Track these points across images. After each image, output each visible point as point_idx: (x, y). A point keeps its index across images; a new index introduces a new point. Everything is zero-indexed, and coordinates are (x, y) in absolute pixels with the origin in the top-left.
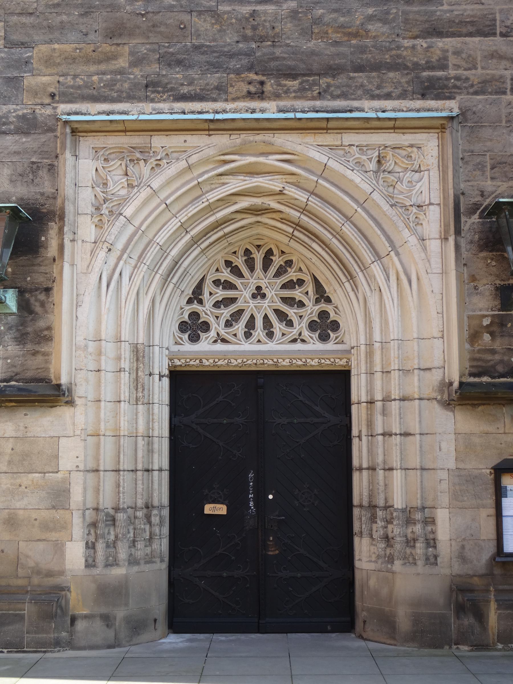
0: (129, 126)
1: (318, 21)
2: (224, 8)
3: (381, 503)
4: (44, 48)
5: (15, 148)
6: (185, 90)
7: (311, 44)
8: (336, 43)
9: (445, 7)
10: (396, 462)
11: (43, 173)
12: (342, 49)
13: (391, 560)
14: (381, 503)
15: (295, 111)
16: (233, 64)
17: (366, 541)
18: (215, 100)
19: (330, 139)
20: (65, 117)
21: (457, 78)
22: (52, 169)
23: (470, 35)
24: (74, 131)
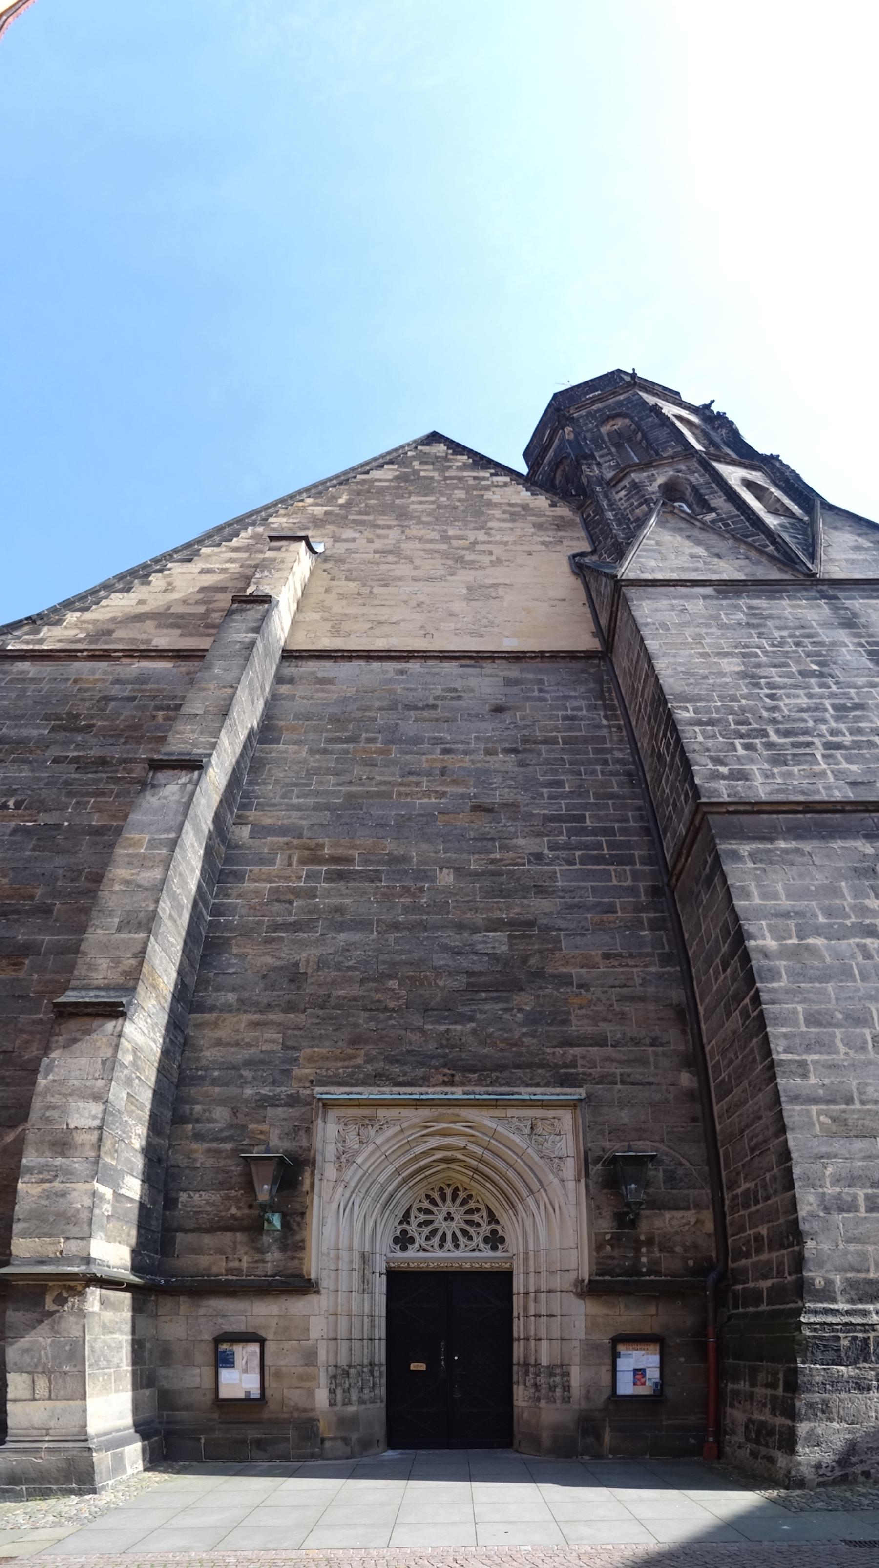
0: (362, 1103)
1: (490, 1036)
2: (428, 1027)
3: (533, 1362)
4: (308, 1051)
5: (284, 1116)
6: (401, 1079)
7: (486, 1050)
8: (502, 1050)
9: (574, 1028)
10: (543, 1334)
11: (302, 1133)
12: (506, 1054)
13: (538, 1399)
14: (533, 1362)
15: (474, 1094)
16: (434, 1062)
17: (521, 1387)
18: (421, 1086)
19: (498, 1113)
20: (319, 1096)
21: (584, 1074)
22: (308, 1131)
23: (591, 1046)
24: (324, 1105)
